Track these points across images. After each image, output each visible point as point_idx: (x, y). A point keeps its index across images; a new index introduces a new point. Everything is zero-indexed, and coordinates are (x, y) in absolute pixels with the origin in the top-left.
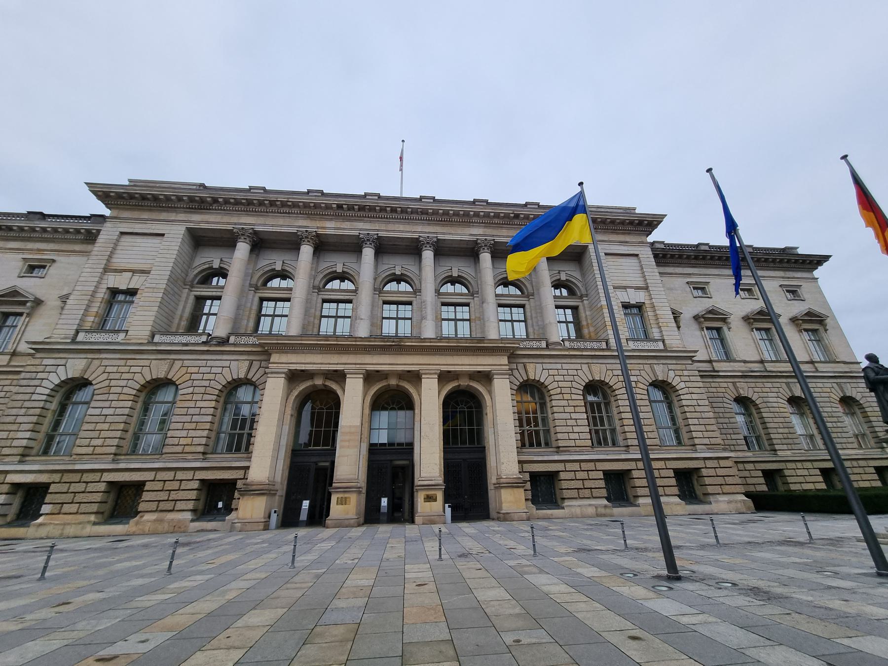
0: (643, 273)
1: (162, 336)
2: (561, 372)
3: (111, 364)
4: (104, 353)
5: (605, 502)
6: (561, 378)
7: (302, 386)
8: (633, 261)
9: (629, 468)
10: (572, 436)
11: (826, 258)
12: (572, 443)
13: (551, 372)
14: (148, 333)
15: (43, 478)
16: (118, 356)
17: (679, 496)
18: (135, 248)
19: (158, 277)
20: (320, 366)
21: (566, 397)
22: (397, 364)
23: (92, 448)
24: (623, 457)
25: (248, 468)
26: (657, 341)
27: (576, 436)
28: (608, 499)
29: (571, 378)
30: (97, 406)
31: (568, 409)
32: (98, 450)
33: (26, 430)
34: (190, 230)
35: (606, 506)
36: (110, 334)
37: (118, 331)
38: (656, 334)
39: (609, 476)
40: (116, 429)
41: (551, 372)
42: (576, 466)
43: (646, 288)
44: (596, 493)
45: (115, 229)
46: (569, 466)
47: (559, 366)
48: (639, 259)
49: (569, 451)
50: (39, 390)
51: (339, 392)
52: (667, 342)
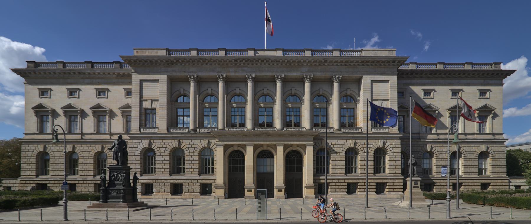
2: (337, 143)
5: (346, 193)
6: (337, 146)
7: (230, 150)
9: (357, 182)
10: (337, 170)
12: (337, 172)
17: (375, 192)
18: (148, 88)
24: (356, 178)
25: (216, 179)
27: (339, 170)
28: (347, 192)
29: (341, 146)
31: (337, 159)
35: (345, 195)
37: (155, 128)
39: (349, 185)
42: (337, 181)
44: (342, 190)
46: (334, 181)
47: (336, 141)
49: (335, 175)
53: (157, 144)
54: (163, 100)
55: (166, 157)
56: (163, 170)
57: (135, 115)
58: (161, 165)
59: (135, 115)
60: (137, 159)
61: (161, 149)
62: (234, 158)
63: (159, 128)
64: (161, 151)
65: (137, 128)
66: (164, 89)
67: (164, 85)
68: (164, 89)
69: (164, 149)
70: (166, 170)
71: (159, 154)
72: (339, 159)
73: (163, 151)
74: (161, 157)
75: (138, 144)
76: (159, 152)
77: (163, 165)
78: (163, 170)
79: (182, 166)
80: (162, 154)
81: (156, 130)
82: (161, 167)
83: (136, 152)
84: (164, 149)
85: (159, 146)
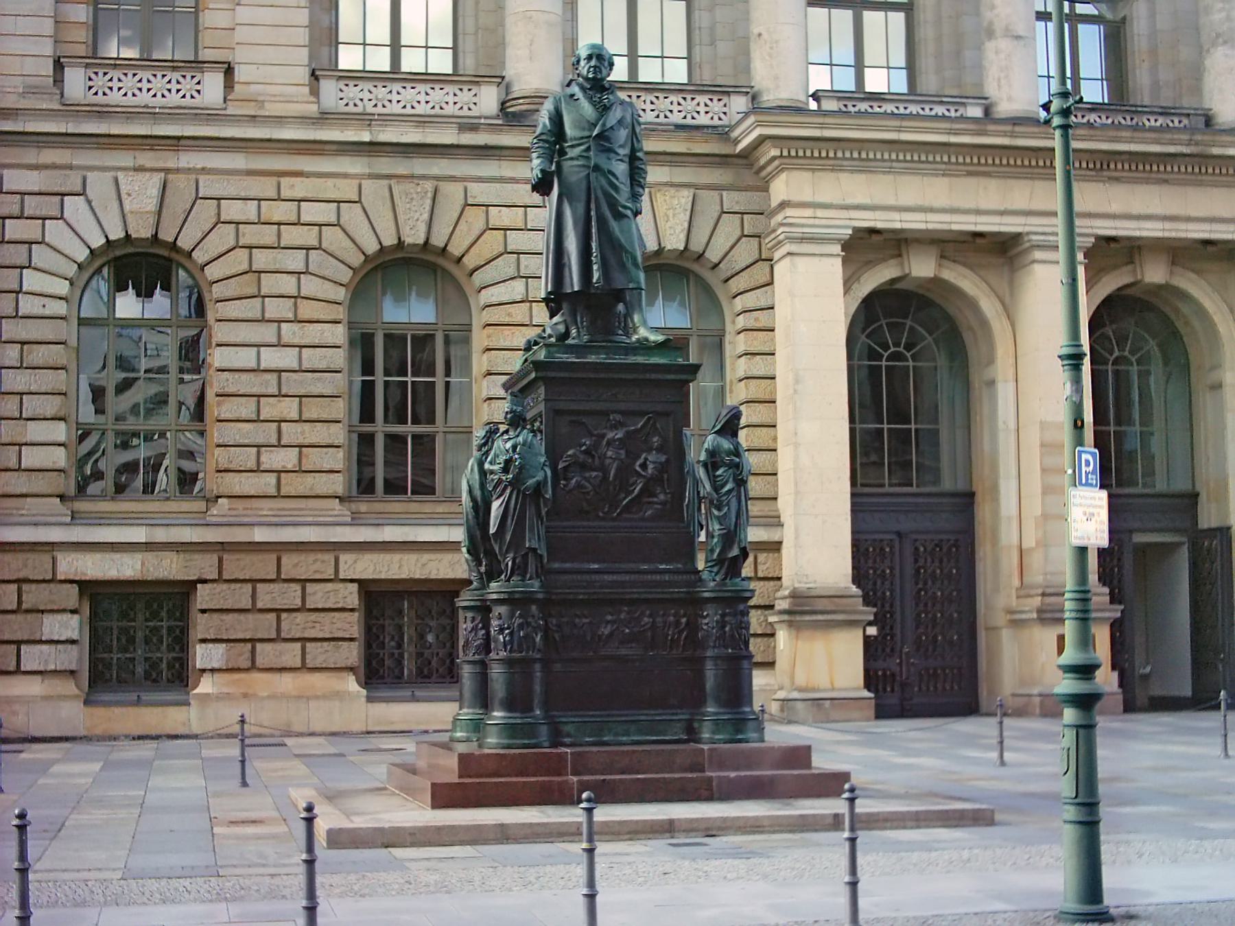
1: (341, 84)
3: (234, 194)
4: (189, 148)
14: (303, 74)
15: (169, 568)
16: (238, 161)
22: (1189, 219)
23: (272, 479)
30: (238, 340)
32: (293, 484)
36: (141, 74)
40: (325, 416)
51: (989, 306)
53: (232, 210)
55: (313, 333)
56: (287, 458)
58: (270, 409)
61: (262, 259)
62: (880, 357)
63: (241, 74)
64: (269, 284)
69: (295, 261)
70: (314, 458)
71: (250, 308)
73: (288, 285)
74: (266, 333)
75: (49, 206)
76: (245, 285)
77: (289, 408)
78: (287, 458)
80: (276, 309)
81: (212, 87)
82: (267, 433)
83: (32, 280)
84: (295, 261)
85: (250, 235)
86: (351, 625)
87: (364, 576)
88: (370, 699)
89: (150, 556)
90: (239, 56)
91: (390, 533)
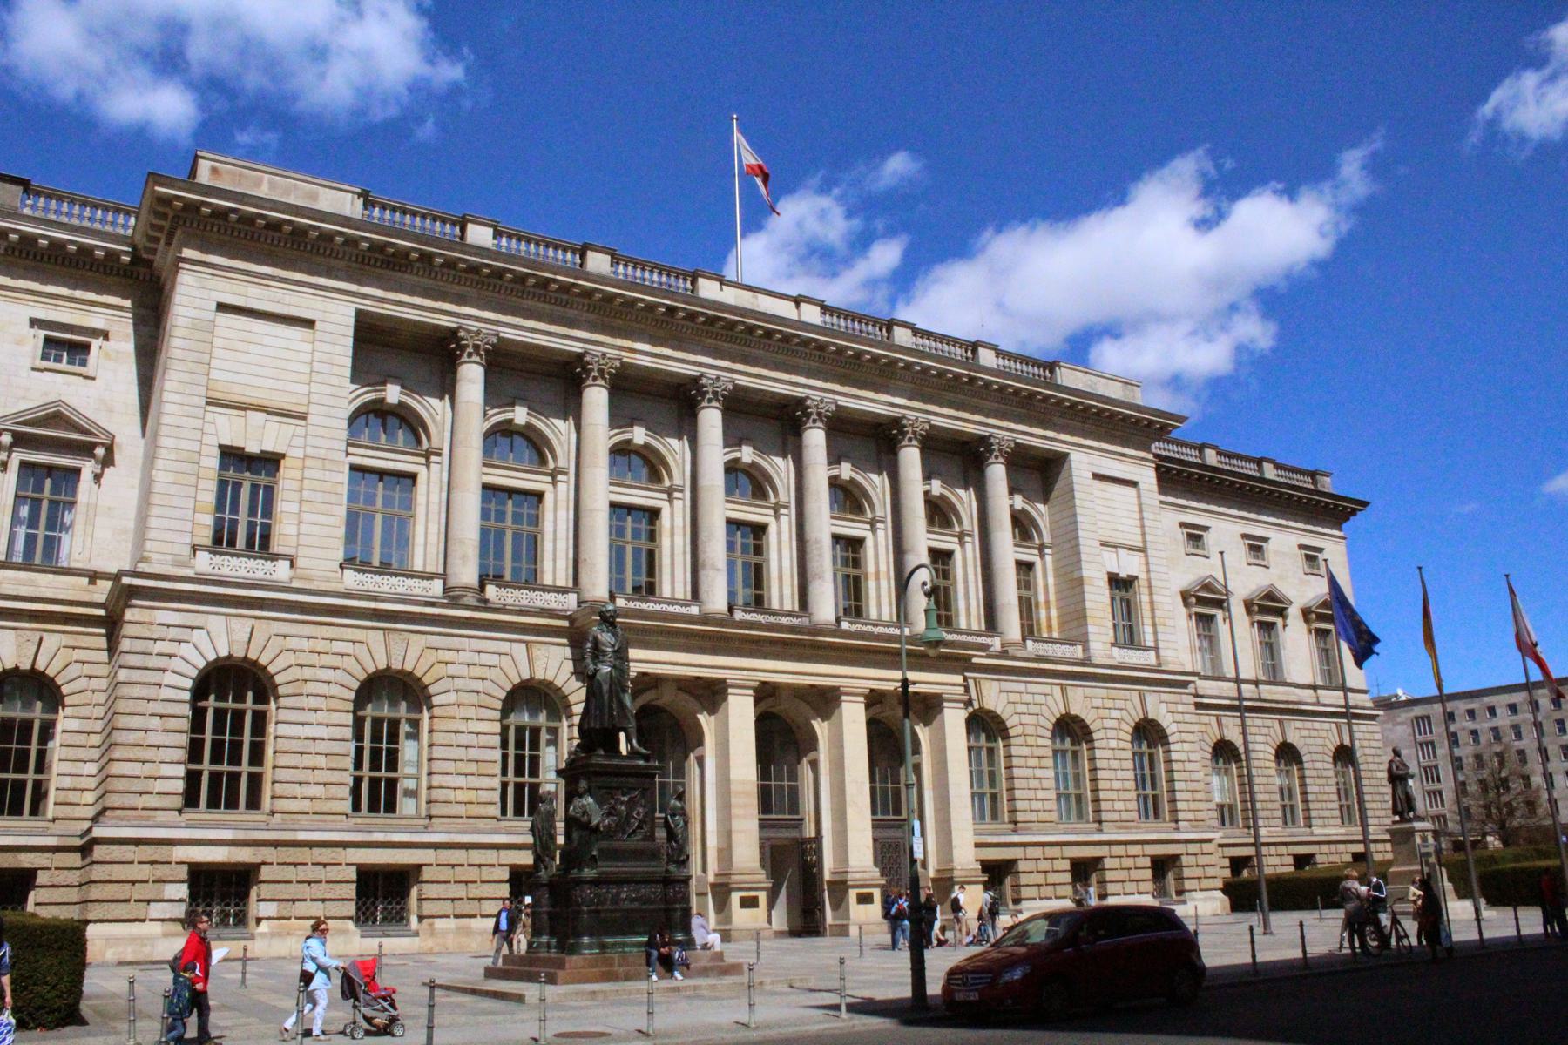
0: (1142, 519)
8: (1131, 491)
11: (1365, 504)
13: (1013, 697)
15: (244, 855)
19: (321, 431)
20: (685, 668)
21: (1030, 740)
26: (1147, 649)
33: (175, 760)
34: (360, 314)
38: (1149, 640)
41: (1013, 697)
43: (1143, 550)
45: (205, 294)
47: (1021, 687)
48: (1139, 491)
50: (168, 678)
52: (1162, 653)
54: (327, 422)
57: (170, 478)
59: (170, 478)
60: (172, 723)
63: (300, 562)
65: (177, 549)
66: (336, 370)
67: (339, 349)
68: (336, 370)
72: (1033, 762)
79: (206, 767)
86: (351, 891)
87: (361, 861)
88: (362, 937)
89: (233, 849)
90: (302, 551)
91: (378, 837)
